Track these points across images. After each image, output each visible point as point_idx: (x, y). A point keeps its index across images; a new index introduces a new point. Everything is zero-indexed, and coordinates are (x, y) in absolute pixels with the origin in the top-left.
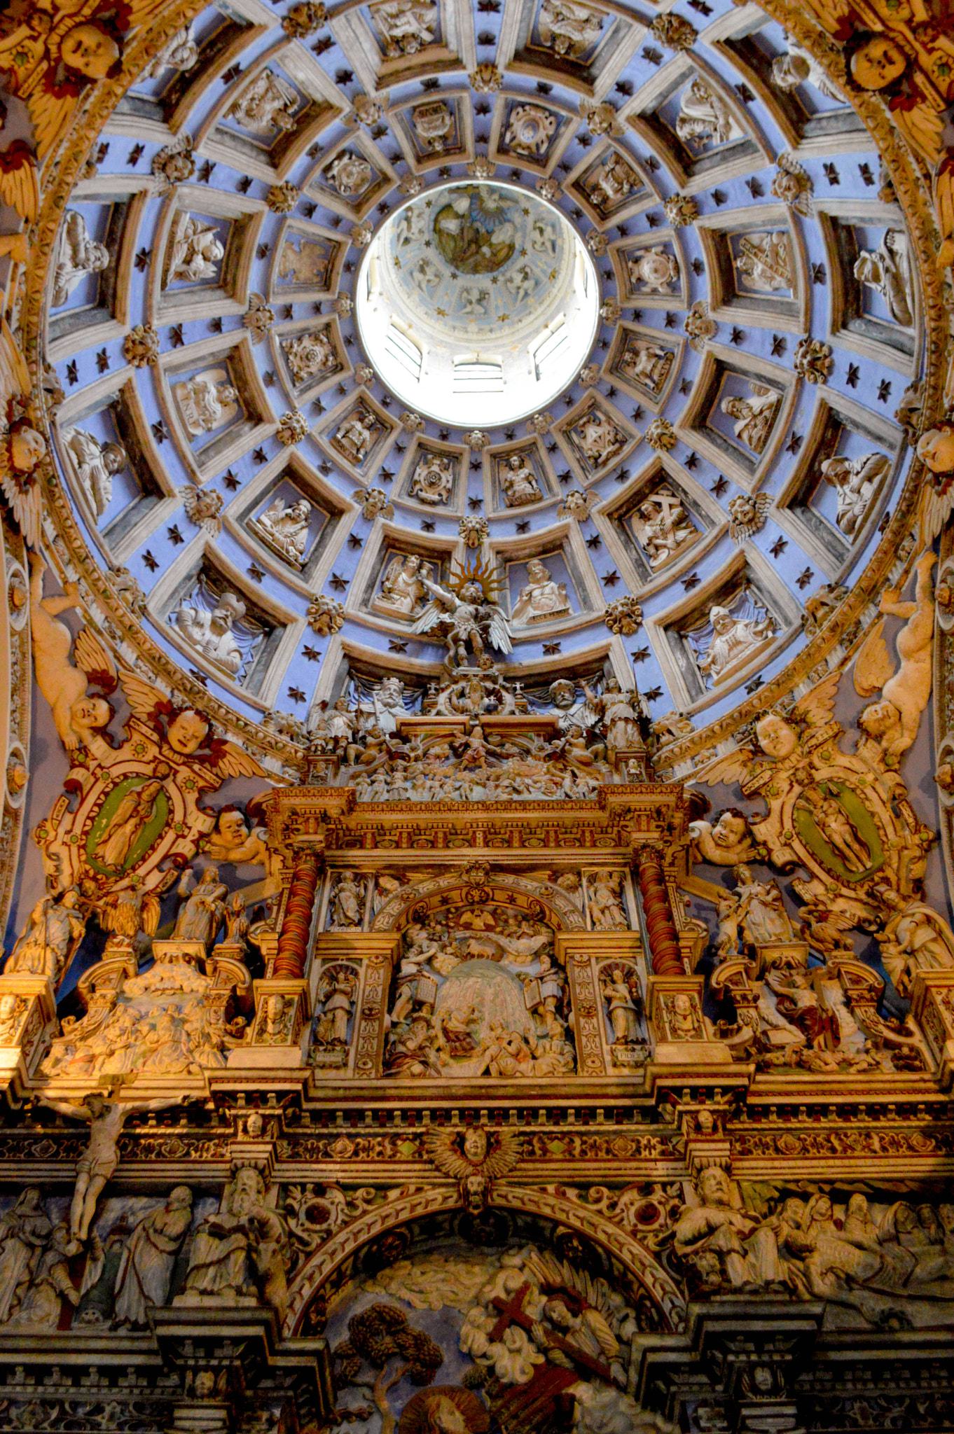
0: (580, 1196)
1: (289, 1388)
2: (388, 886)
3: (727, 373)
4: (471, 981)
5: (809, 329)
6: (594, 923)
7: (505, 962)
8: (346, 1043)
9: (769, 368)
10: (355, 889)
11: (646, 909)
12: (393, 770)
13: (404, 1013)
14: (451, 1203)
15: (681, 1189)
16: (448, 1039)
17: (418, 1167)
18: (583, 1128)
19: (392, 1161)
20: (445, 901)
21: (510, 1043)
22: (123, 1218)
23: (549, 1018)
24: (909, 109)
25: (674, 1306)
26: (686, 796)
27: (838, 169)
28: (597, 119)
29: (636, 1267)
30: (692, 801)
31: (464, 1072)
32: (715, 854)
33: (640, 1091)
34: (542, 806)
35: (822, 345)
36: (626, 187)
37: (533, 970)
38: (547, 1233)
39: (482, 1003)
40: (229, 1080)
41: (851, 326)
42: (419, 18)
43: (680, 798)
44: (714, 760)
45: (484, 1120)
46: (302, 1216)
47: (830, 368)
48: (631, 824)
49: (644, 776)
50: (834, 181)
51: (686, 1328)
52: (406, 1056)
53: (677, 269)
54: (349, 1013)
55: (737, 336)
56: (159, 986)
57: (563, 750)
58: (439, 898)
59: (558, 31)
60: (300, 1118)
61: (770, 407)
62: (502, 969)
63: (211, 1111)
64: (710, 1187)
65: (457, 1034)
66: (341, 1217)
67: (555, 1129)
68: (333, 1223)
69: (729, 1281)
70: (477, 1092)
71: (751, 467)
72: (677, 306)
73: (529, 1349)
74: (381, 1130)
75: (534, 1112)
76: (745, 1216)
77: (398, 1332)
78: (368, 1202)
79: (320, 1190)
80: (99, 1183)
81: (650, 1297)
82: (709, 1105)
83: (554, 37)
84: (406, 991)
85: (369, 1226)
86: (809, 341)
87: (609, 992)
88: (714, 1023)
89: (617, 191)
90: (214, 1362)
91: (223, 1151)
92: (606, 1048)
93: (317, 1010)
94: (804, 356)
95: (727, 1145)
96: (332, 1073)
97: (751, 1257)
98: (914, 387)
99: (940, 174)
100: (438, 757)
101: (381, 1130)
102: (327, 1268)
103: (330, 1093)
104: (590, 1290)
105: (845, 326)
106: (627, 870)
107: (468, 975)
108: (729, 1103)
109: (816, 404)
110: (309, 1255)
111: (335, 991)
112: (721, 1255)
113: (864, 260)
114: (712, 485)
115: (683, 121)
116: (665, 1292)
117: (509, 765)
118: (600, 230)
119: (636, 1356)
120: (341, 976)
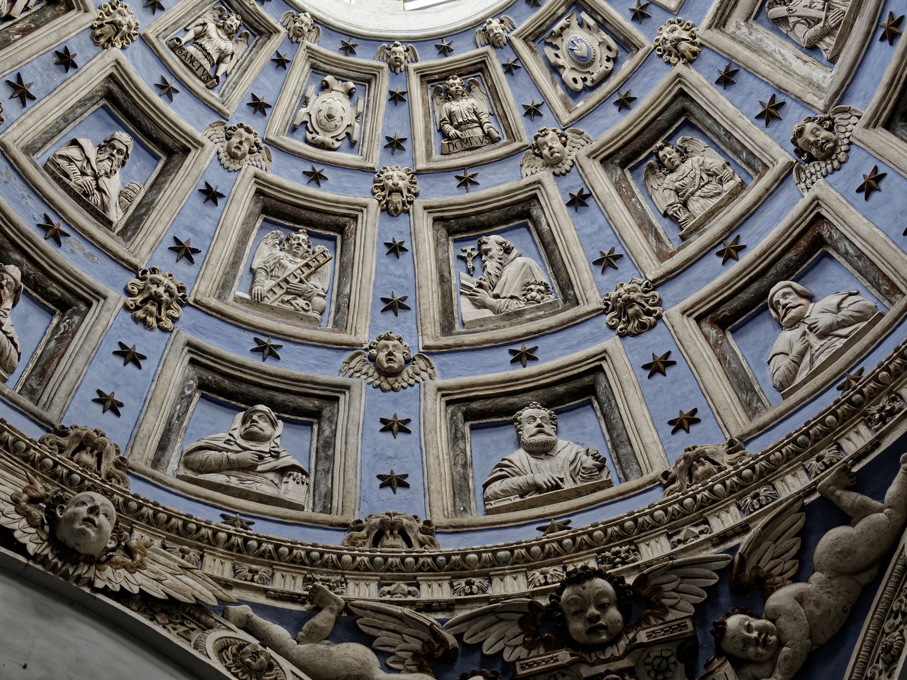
3: (164, 159)
5: (198, 305)
9: (159, 228)
24: (521, 623)
27: (401, 437)
28: (557, 145)
35: (174, 320)
36: (453, 132)
41: (192, 372)
42: (810, 22)
47: (144, 321)
50: (388, 426)
53: (322, 146)
55: (211, 195)
59: (689, 162)
61: (105, 207)
71: (30, 150)
72: (275, 126)
83: (684, 154)
86: (183, 302)
89: (451, 115)
94: (168, 290)
98: (121, 464)
99: (431, 629)
105: (192, 362)
109: (101, 286)
113: (274, 424)
114: (26, 80)
115: (507, 250)
118: (412, 66)
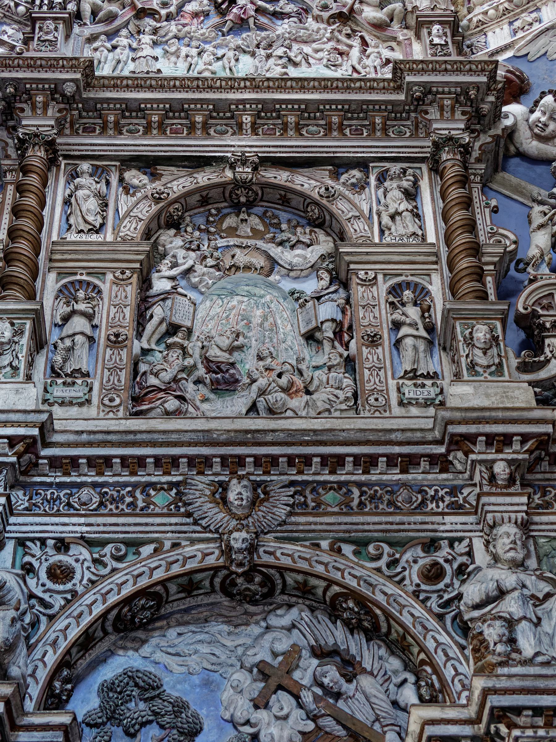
0: (355, 553)
2: (135, 182)
4: (235, 301)
6: (382, 232)
7: (274, 277)
8: (88, 375)
10: (94, 186)
11: (445, 217)
12: (139, 32)
13: (156, 336)
14: (211, 561)
15: (470, 546)
16: (209, 370)
17: (174, 520)
18: (363, 478)
19: (144, 512)
20: (205, 201)
21: (280, 375)
23: (327, 345)
25: (457, 673)
26: (501, 72)
29: (417, 631)
30: (508, 81)
31: (225, 413)
32: (533, 146)
33: (429, 437)
34: (324, 84)
37: (310, 286)
38: (320, 592)
39: (248, 325)
43: (492, 76)
44: (537, 27)
45: (250, 469)
46: (43, 575)
48: (431, 110)
49: (451, 48)
51: (469, 699)
52: (160, 390)
54: (91, 339)
57: (352, 10)
58: (197, 197)
60: (36, 465)
62: (272, 286)
64: (502, 545)
65: (218, 364)
66: (87, 575)
67: (332, 478)
68: (77, 583)
69: (519, 651)
70: (240, 437)
73: (298, 713)
74: (133, 479)
75: (307, 460)
76: (541, 578)
77: (152, 698)
78: (119, 559)
79: (62, 545)
81: (432, 664)
82: (508, 454)
84: (158, 312)
87: (397, 316)
88: (518, 356)
92: (392, 384)
93: (53, 336)
95: (525, 499)
96: (74, 411)
97: (546, 626)
100: (196, 15)
101: (133, 479)
102: (74, 633)
103: (72, 438)
104: (366, 653)
106: (424, 167)
107: (233, 293)
108: (530, 452)
110: (51, 618)
111: (74, 312)
112: (511, 623)
116: (448, 658)
117: (283, 27)
119: (414, 727)
120: (81, 294)
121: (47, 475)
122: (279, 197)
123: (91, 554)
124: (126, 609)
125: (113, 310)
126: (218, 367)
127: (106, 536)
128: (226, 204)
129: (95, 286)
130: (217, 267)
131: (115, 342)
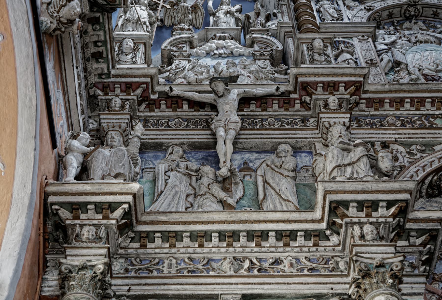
1: (420, 245)
4: (427, 53)
20: (390, 15)
22: (245, 163)
40: (309, 75)
56: (216, 52)
58: (387, 13)
63: (295, 99)
78: (422, 151)
80: (232, 134)
85: (431, 163)
90: (371, 220)
91: (308, 125)
101: (418, 112)
103: (380, 88)
107: (425, 50)
121: (364, 111)
122: (432, 13)
123: (405, 149)
124: (435, 178)
125: (364, 53)
126: (433, 78)
127: (411, 139)
128: (401, 19)
129: (348, 43)
130: (409, 41)
131: (371, 64)
